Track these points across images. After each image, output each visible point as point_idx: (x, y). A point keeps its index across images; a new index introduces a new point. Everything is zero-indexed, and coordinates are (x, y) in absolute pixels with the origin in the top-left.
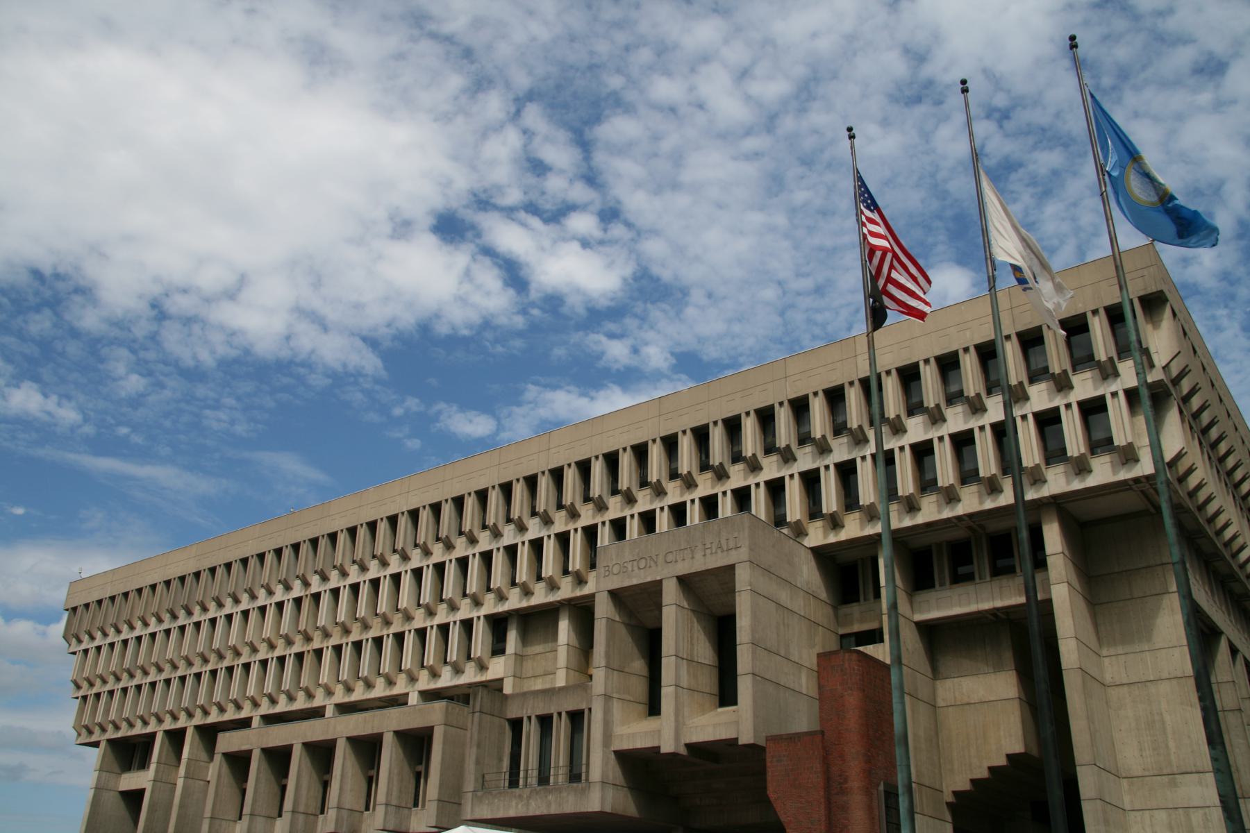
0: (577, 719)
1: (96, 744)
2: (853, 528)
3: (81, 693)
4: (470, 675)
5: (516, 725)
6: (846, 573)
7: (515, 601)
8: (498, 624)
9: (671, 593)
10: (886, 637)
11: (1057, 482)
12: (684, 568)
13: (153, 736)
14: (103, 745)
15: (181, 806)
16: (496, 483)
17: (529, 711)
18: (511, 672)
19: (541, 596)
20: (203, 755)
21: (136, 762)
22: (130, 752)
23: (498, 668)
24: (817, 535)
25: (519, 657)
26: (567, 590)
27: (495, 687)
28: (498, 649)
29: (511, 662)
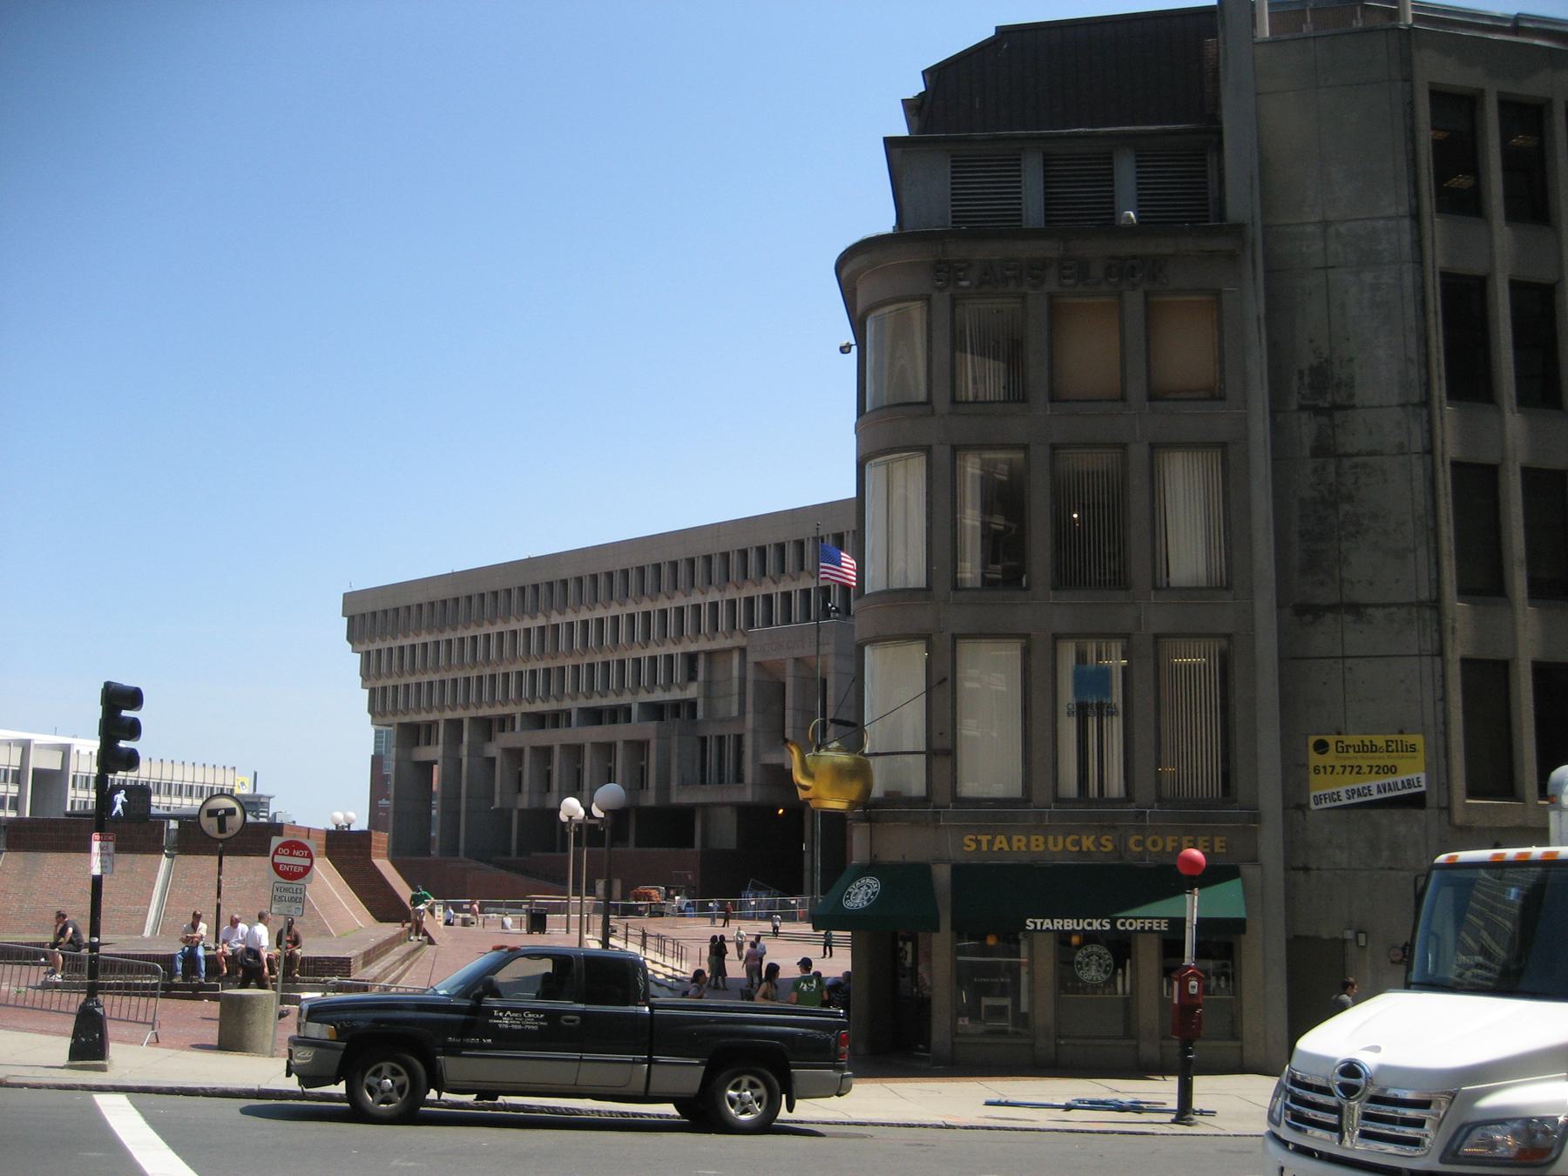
0: (739, 739)
4: (675, 695)
5: (704, 740)
7: (702, 645)
8: (691, 658)
9: (790, 668)
12: (798, 653)
13: (436, 722)
15: (468, 777)
17: (711, 731)
19: (720, 643)
21: (422, 740)
23: (693, 691)
25: (709, 684)
27: (692, 705)
28: (692, 676)
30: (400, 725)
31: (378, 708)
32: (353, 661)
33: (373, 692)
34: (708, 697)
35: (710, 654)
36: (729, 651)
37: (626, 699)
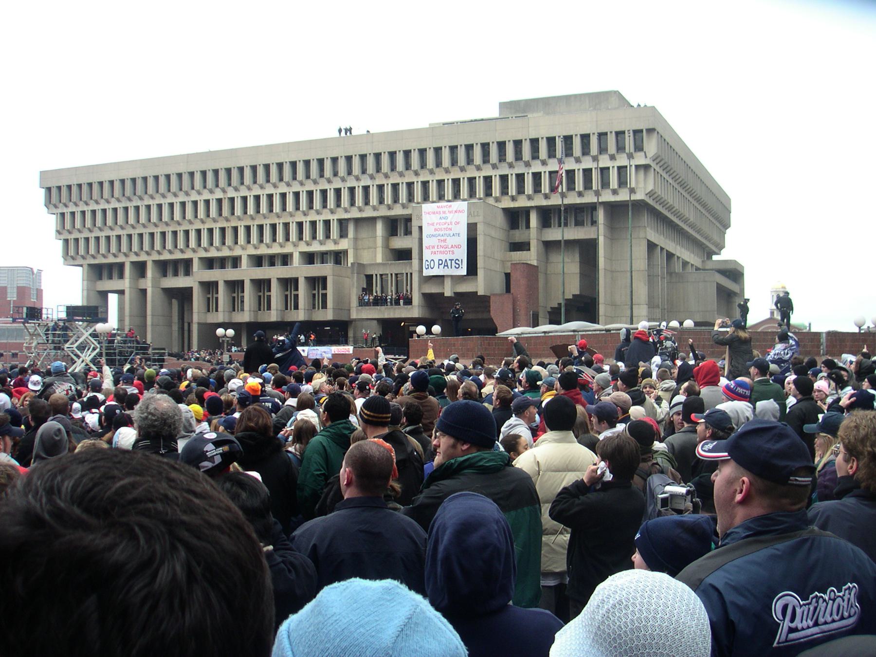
1: (81, 266)
2: (522, 202)
3: (63, 237)
4: (330, 246)
6: (515, 218)
7: (355, 214)
8: (343, 224)
10: (532, 248)
11: (607, 197)
13: (121, 266)
14: (86, 267)
16: (343, 155)
18: (352, 246)
19: (368, 213)
20: (157, 275)
22: (99, 271)
23: (344, 244)
24: (507, 203)
25: (356, 239)
26: (383, 212)
28: (343, 234)
29: (352, 242)
30: (90, 265)
31: (72, 252)
32: (51, 221)
33: (66, 241)
34: (356, 249)
35: (358, 222)
36: (373, 220)
37: (288, 249)
